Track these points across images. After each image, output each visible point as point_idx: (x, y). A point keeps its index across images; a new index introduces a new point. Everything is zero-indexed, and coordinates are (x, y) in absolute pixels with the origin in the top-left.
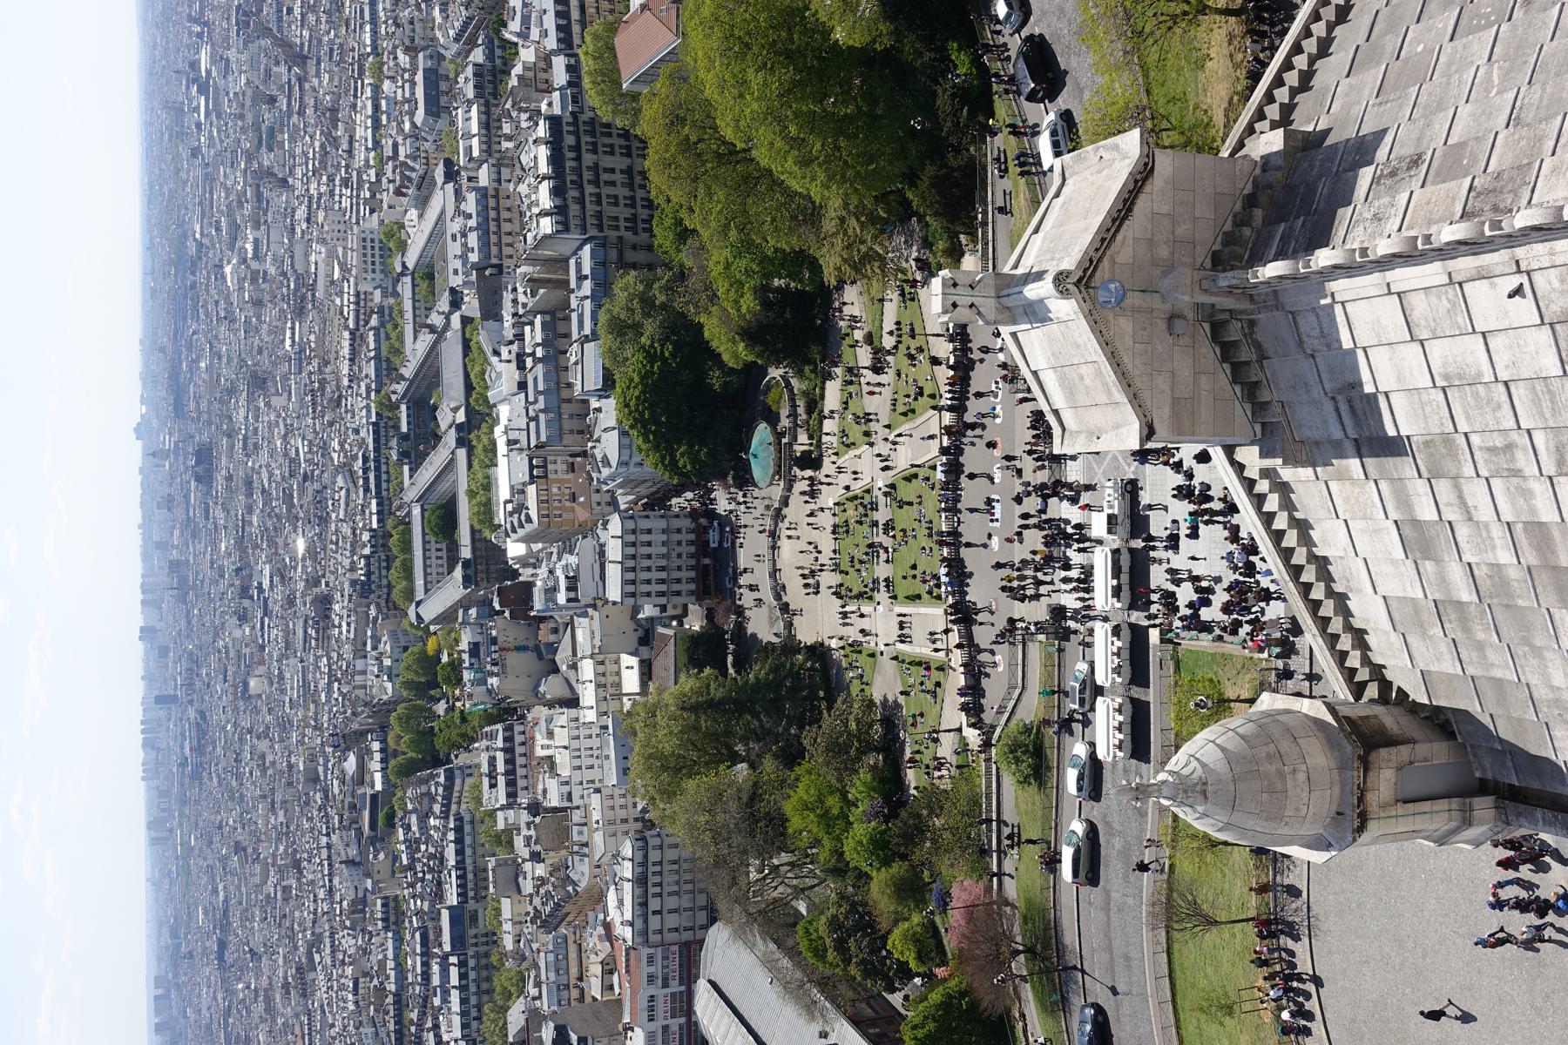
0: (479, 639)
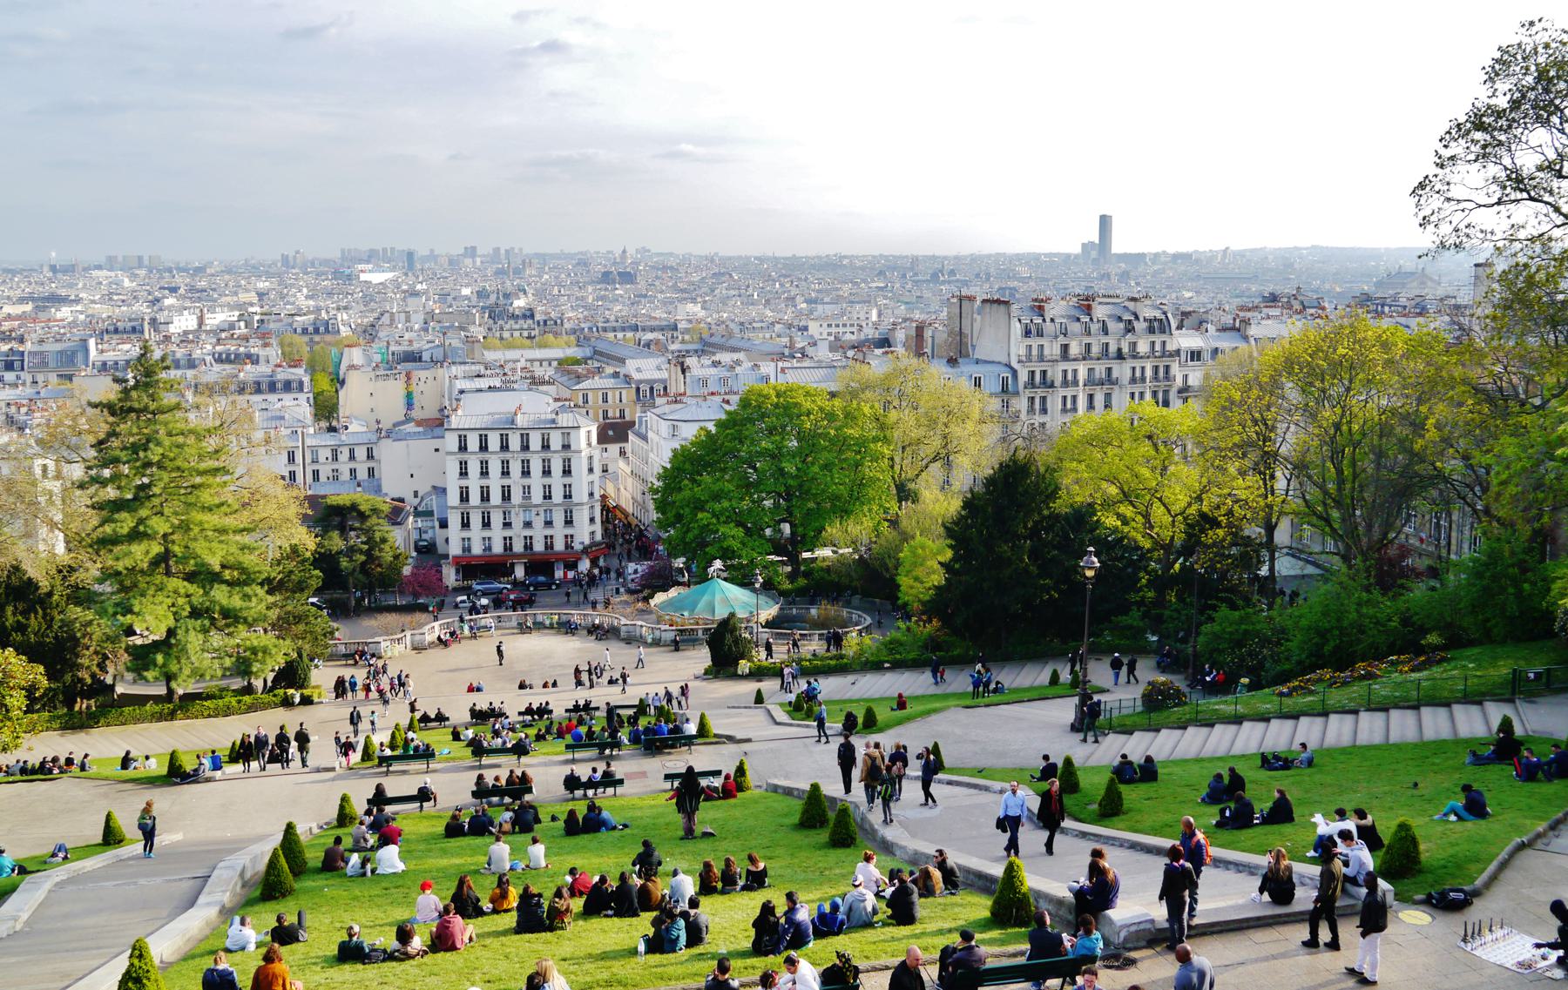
0: (426, 356)
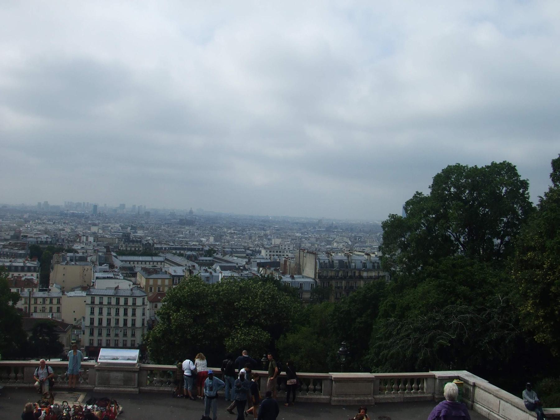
0: (89, 259)
